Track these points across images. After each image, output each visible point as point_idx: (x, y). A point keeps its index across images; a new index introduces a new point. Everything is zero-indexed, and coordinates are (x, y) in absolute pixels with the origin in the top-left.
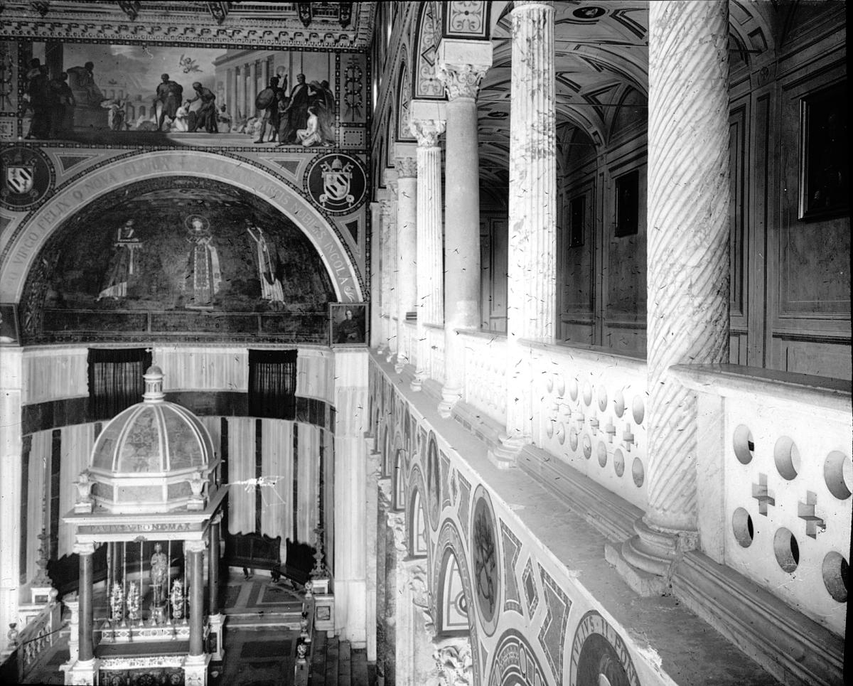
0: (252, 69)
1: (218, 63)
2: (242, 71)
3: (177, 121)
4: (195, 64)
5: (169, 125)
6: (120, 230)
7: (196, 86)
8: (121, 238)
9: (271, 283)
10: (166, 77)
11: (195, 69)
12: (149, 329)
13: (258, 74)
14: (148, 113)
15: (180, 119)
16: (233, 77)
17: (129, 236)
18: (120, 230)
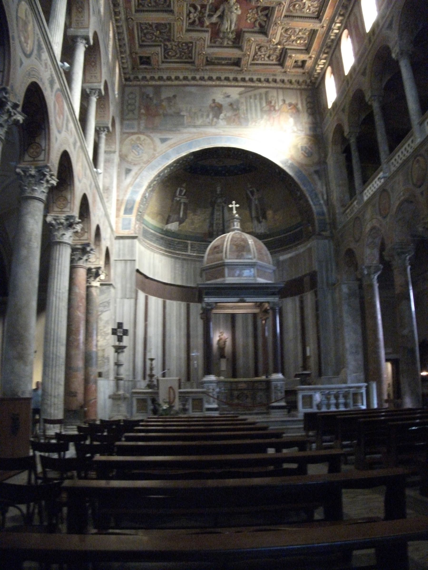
0: (258, 97)
1: (240, 94)
2: (253, 97)
3: (220, 121)
4: (229, 94)
5: (216, 122)
6: (179, 189)
7: (229, 104)
9: (260, 222)
10: (214, 101)
11: (228, 96)
12: (189, 250)
13: (261, 99)
14: (205, 117)
15: (222, 119)
16: (248, 100)
17: (183, 194)
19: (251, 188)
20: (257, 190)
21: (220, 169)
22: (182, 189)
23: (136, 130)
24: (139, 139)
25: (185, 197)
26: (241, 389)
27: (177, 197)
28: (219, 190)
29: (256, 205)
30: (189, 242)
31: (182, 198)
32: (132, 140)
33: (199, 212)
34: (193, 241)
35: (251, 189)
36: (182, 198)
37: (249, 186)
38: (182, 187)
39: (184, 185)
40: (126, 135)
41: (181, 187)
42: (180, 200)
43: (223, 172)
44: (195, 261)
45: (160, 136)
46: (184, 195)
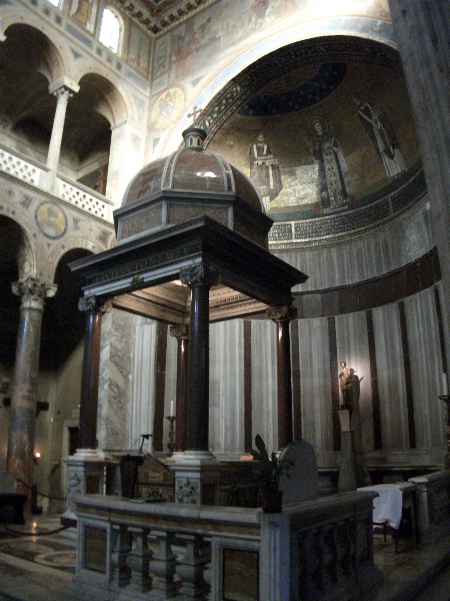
6: (255, 146)
8: (259, 155)
17: (265, 152)
18: (255, 146)
19: (361, 105)
20: (372, 105)
21: (302, 93)
22: (260, 145)
23: (166, 86)
24: (168, 95)
25: (269, 156)
26: (154, 484)
27: (257, 159)
28: (318, 127)
29: (380, 131)
30: (293, 223)
31: (266, 159)
32: (162, 100)
33: (299, 170)
34: (298, 220)
35: (362, 108)
36: (266, 159)
37: (358, 103)
38: (262, 143)
39: (261, 138)
40: (156, 97)
41: (258, 142)
42: (264, 163)
43: (310, 96)
44: (302, 250)
45: (191, 79)
46: (269, 152)
